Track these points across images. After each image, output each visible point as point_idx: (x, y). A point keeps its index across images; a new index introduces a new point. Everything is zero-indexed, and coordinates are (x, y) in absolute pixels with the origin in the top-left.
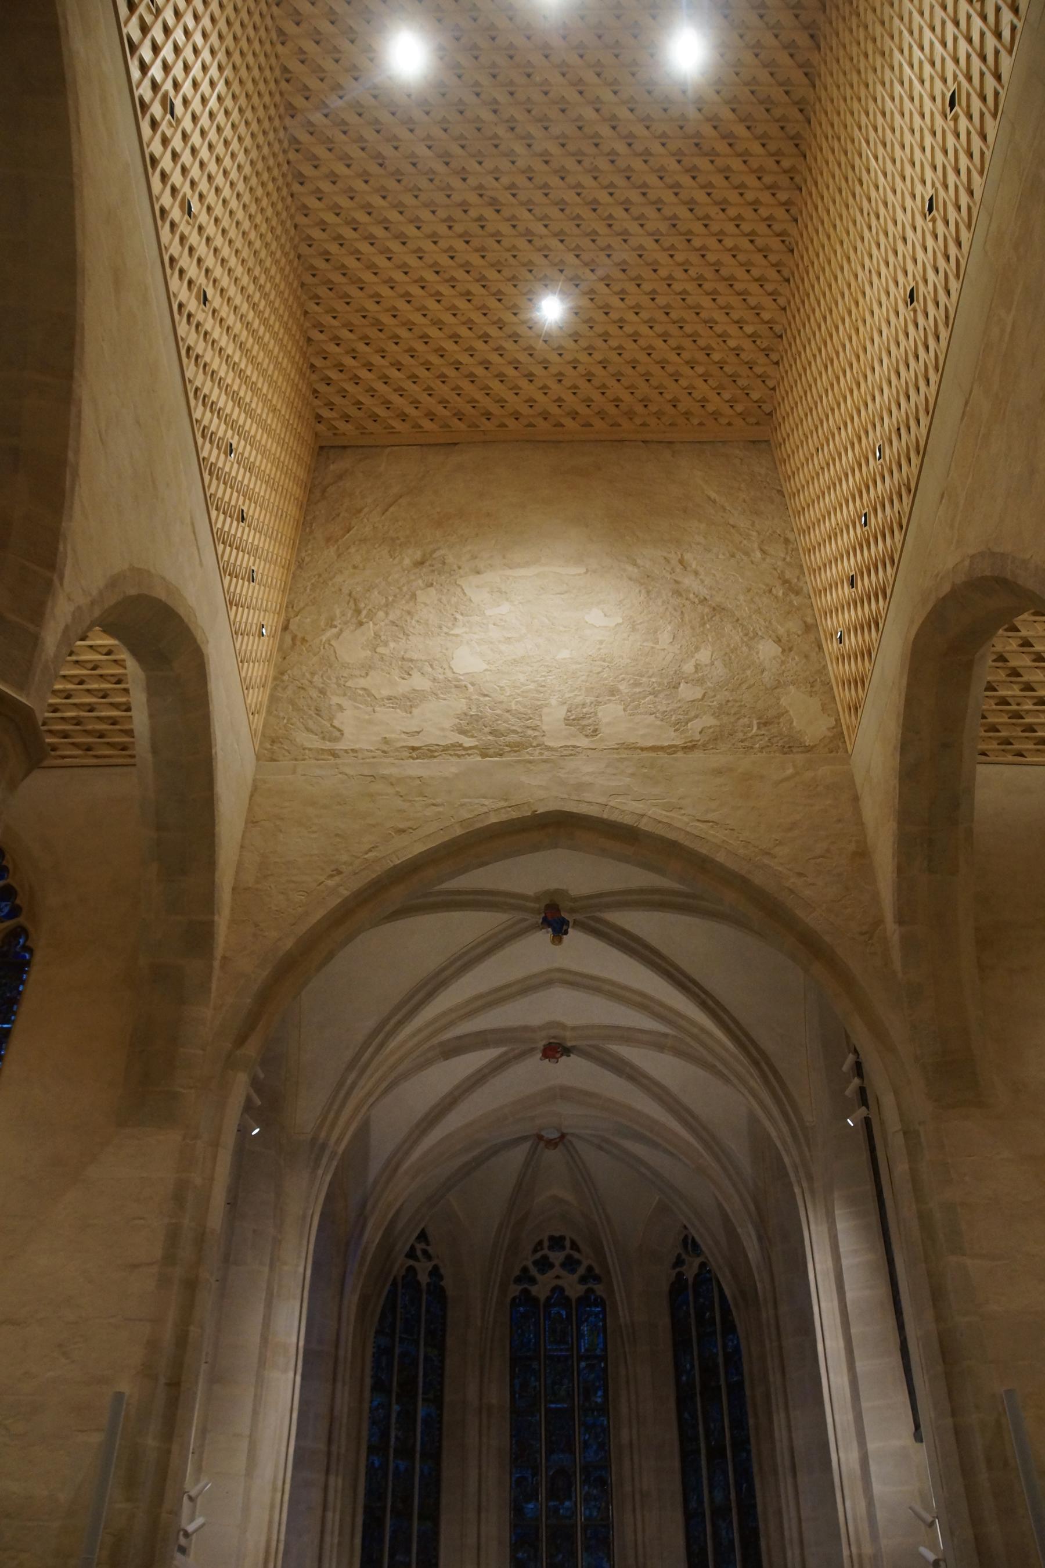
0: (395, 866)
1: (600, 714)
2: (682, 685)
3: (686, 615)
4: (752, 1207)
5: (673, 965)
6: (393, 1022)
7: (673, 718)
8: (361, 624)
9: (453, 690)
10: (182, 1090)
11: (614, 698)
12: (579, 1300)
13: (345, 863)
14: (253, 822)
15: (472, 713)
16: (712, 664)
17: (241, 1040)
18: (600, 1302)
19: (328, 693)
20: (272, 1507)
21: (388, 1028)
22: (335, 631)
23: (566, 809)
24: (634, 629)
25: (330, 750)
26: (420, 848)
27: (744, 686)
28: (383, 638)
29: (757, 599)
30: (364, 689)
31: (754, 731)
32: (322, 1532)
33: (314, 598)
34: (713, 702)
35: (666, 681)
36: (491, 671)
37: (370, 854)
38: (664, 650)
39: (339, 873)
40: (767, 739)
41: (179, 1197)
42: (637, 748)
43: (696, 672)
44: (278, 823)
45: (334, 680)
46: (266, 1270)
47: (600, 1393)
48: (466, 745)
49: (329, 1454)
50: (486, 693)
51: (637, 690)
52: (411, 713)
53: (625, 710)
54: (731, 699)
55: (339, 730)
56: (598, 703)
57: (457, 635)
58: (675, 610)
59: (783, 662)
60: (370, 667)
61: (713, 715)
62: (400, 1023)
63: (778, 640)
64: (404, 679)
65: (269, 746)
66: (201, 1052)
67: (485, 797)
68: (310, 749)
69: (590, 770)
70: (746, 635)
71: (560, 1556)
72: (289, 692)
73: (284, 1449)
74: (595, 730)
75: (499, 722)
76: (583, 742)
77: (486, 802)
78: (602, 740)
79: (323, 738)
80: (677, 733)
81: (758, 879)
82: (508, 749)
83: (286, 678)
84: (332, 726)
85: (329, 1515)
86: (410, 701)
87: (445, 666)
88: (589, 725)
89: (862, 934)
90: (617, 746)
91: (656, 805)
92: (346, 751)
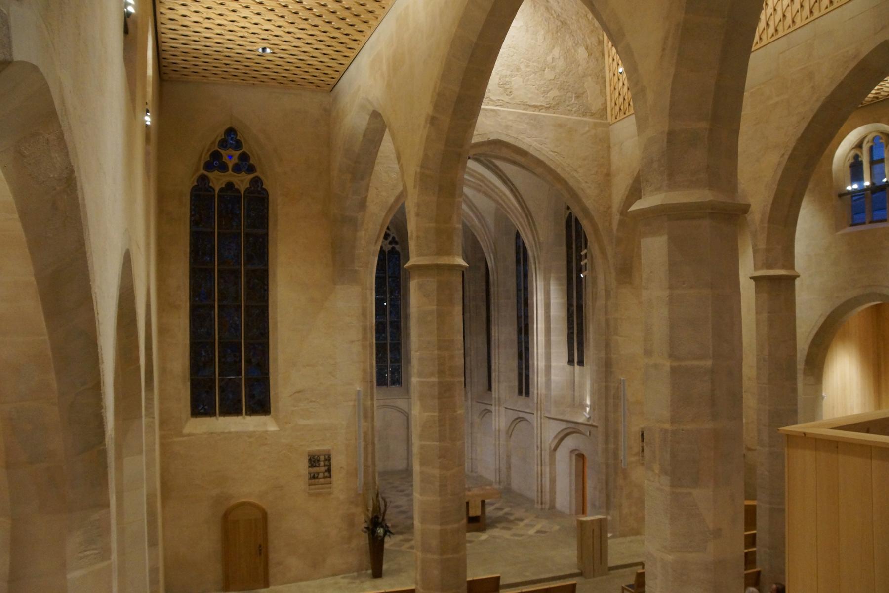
1: (513, 83)
2: (546, 69)
3: (550, 25)
4: (493, 247)
5: (504, 174)
7: (542, 89)
11: (518, 73)
12: (389, 251)
16: (559, 58)
18: (398, 253)
24: (527, 31)
27: (571, 73)
29: (580, 20)
31: (573, 101)
34: (558, 81)
35: (540, 66)
38: (540, 46)
40: (578, 106)
42: (527, 105)
43: (552, 62)
47: (397, 292)
51: (528, 69)
53: (523, 82)
54: (565, 80)
56: (511, 76)
58: (546, 21)
59: (588, 62)
61: (558, 89)
63: (587, 49)
66: (362, 251)
69: (511, 118)
70: (574, 42)
71: (380, 355)
74: (511, 92)
76: (506, 99)
78: (513, 98)
80: (543, 99)
81: (571, 182)
88: (508, 89)
89: (605, 212)
90: (519, 103)
91: (536, 141)
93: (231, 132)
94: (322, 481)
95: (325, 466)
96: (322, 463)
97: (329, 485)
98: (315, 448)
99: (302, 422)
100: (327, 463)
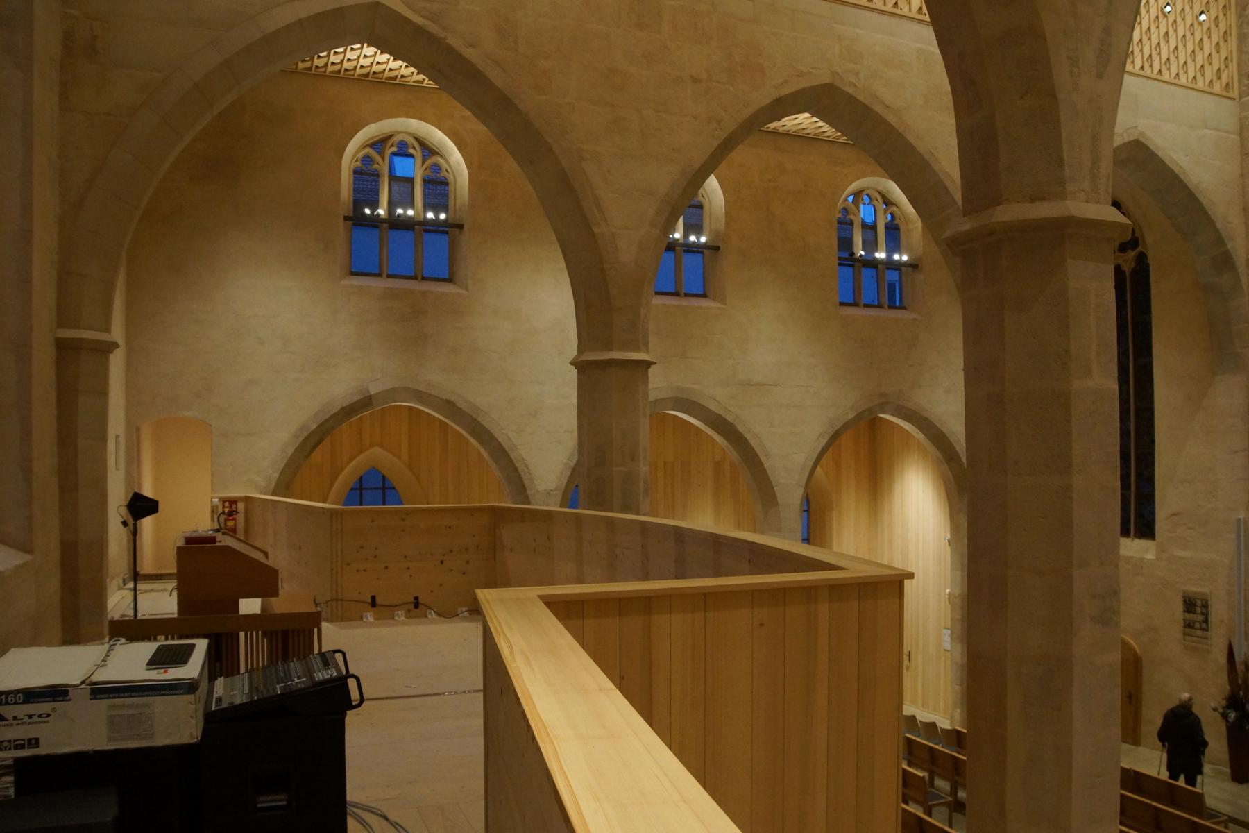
94: (1199, 633)
95: (1202, 614)
96: (1199, 610)
97: (1205, 641)
98: (1192, 588)
99: (1180, 553)
100: (1204, 610)
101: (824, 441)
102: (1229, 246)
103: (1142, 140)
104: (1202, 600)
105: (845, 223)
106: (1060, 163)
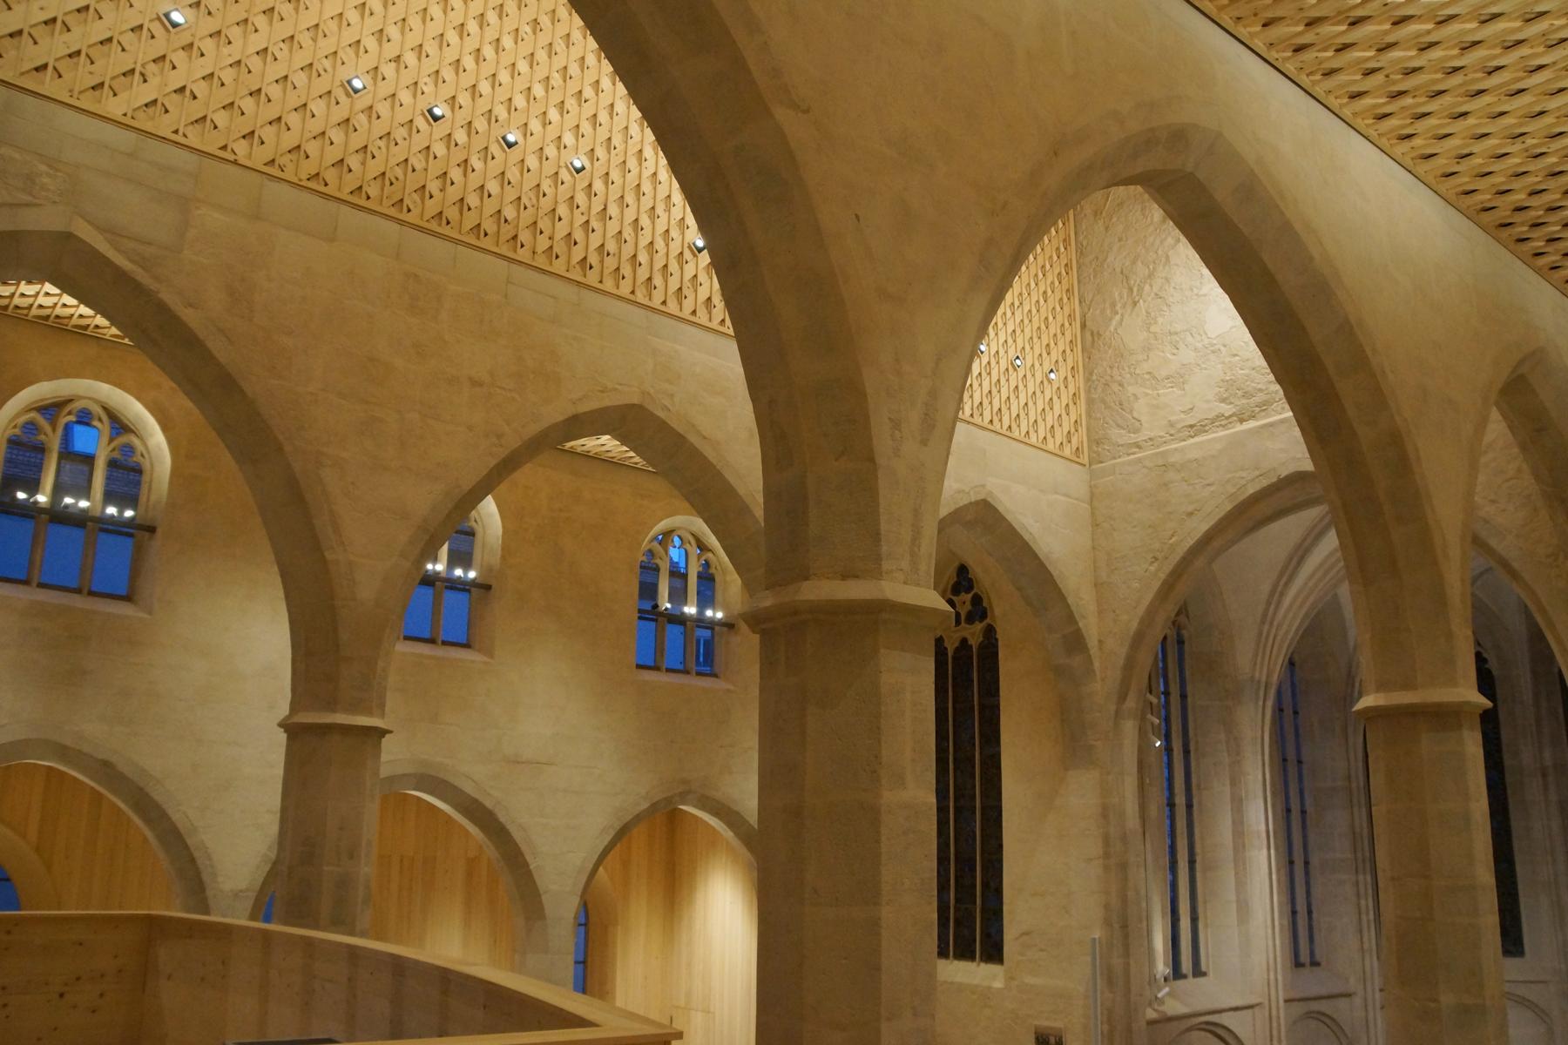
0: (1190, 547)
6: (1282, 583)
8: (1135, 303)
9: (1212, 357)
10: (1095, 743)
13: (1158, 551)
14: (1097, 525)
15: (1228, 378)
17: (1122, 697)
19: (1125, 385)
20: (1267, 938)
21: (1279, 589)
22: (1118, 317)
23: (1302, 469)
25: (1135, 443)
26: (1205, 527)
28: (1153, 314)
30: (1149, 373)
32: (1360, 914)
33: (1098, 285)
36: (1235, 327)
37: (1174, 539)
39: (1156, 559)
41: (1105, 812)
44: (1112, 523)
45: (1127, 369)
46: (1227, 789)
48: (1226, 415)
49: (1356, 859)
50: (1235, 352)
52: (1184, 390)
55: (1139, 421)
57: (1205, 295)
60: (1149, 349)
62: (1286, 584)
64: (1174, 355)
65: (1096, 449)
67: (1242, 470)
68: (1122, 445)
72: (1100, 390)
73: (1268, 901)
75: (1248, 383)
77: (1244, 474)
79: (1129, 432)
82: (1258, 409)
83: (1094, 377)
84: (1134, 418)
85: (1363, 902)
86: (1182, 377)
87: (1202, 333)
92: (1146, 441)
93: (963, 570)
98: (1044, 1023)
99: (1030, 980)
101: (607, 839)
102: (1081, 625)
103: (989, 499)
104: (1056, 1037)
105: (649, 570)
106: (876, 537)
